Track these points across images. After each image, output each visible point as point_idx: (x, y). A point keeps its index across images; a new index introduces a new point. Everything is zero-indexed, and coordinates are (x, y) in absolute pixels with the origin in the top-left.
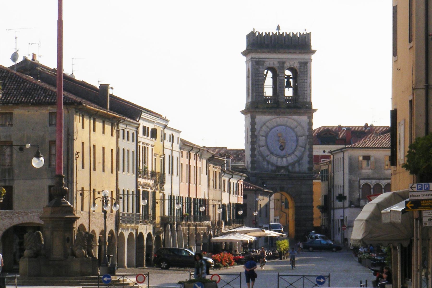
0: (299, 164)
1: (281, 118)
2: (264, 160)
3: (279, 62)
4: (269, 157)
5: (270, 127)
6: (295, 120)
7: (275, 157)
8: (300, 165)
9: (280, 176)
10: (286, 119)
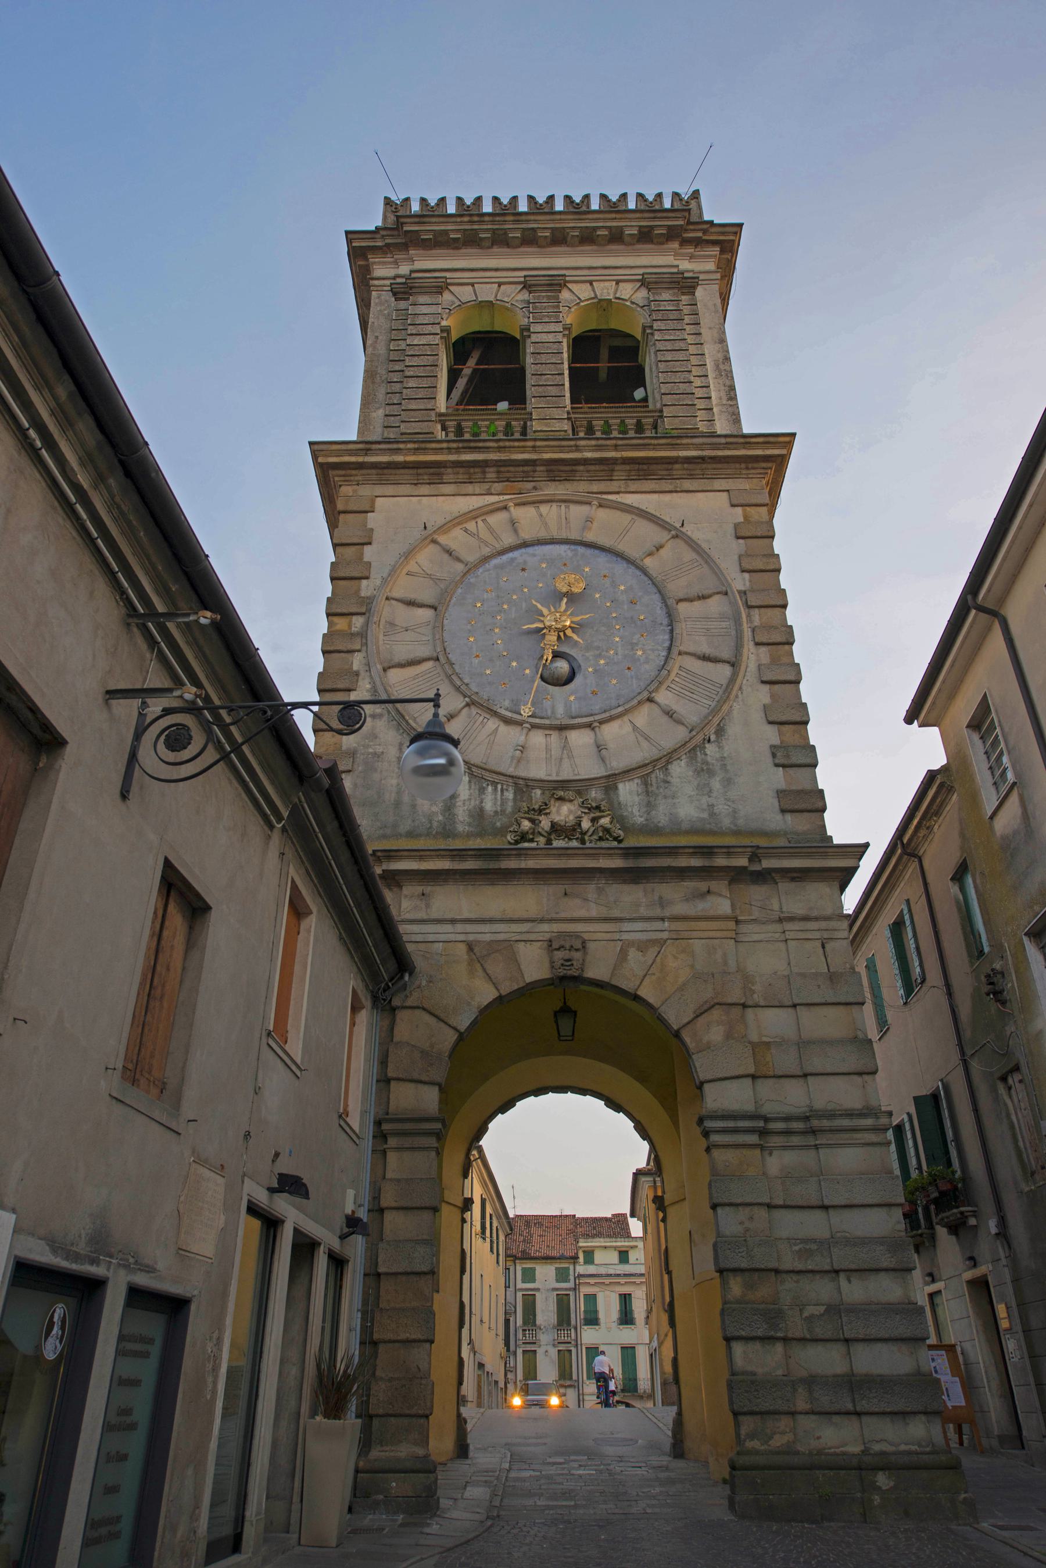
0: (704, 771)
1: (544, 509)
7: (503, 728)
8: (711, 773)
9: (549, 842)
10: (577, 512)
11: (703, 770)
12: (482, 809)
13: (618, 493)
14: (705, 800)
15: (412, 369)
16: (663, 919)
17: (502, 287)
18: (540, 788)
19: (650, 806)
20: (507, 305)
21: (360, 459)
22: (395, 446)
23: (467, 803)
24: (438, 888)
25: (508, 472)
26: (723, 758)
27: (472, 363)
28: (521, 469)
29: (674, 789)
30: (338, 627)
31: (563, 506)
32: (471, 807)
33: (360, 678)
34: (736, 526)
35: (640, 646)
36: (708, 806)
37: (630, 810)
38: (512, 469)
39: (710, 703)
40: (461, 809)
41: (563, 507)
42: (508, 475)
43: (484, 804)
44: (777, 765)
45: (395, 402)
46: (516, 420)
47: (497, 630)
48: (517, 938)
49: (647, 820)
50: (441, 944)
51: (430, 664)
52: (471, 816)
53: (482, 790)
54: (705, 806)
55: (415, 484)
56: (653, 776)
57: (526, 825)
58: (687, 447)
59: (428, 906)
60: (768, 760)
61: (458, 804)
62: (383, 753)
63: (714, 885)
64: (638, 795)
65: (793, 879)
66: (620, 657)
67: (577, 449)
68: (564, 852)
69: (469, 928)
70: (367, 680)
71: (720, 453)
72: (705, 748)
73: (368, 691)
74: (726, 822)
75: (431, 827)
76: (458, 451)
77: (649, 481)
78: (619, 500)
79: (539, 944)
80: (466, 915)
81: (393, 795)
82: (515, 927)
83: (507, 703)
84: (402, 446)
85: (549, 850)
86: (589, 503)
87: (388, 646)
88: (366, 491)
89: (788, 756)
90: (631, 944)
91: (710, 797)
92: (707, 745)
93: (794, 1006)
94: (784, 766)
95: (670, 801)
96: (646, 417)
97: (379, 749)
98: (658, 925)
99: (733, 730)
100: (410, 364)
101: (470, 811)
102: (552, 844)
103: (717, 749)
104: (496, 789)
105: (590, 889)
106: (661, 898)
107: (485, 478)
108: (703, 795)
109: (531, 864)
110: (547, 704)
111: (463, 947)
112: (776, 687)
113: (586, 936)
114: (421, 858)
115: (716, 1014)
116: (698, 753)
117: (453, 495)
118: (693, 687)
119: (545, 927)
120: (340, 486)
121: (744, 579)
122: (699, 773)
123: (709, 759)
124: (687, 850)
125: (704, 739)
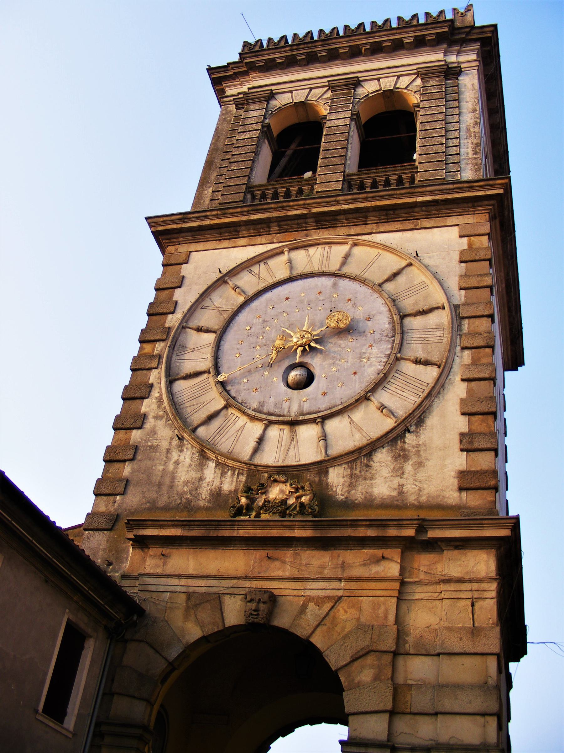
1: (312, 250)
2: (181, 439)
3: (332, 87)
4: (216, 423)
5: (251, 292)
6: (386, 248)
8: (406, 458)
9: (258, 515)
11: (399, 455)
12: (220, 489)
13: (370, 234)
14: (396, 481)
15: (236, 156)
16: (340, 580)
17: (313, 91)
18: (267, 472)
19: (352, 486)
20: (314, 102)
21: (179, 226)
22: (204, 214)
23: (210, 484)
24: (174, 551)
25: (286, 225)
26: (418, 446)
27: (293, 147)
28: (296, 222)
29: (373, 471)
30: (146, 351)
31: (327, 246)
32: (213, 487)
33: (153, 389)
34: (462, 253)
35: (367, 355)
36: (399, 485)
37: (334, 489)
38: (289, 222)
39: (416, 399)
40: (205, 489)
41: (327, 248)
42: (286, 227)
43: (222, 485)
44: (462, 450)
45: (221, 182)
46: (305, 185)
47: (258, 348)
48: (225, 592)
49: (346, 498)
50: (169, 593)
51: (206, 376)
52: (211, 494)
53: (223, 474)
54: (396, 486)
55: (220, 240)
56: (359, 461)
57: (243, 500)
58: (424, 194)
59: (164, 564)
60: (456, 445)
61: (204, 485)
62: (157, 445)
63: (388, 552)
64: (343, 477)
65: (457, 548)
66: (349, 364)
67: (338, 203)
68: (266, 524)
69: (191, 582)
70: (158, 390)
71: (450, 196)
72: (405, 436)
73: (156, 398)
74: (412, 499)
75: (180, 503)
76: (249, 213)
77: (396, 223)
78: (370, 240)
79: (241, 596)
80: (191, 571)
81: (158, 478)
82: (225, 583)
83: (255, 405)
84: (208, 213)
85: (258, 523)
86: (347, 244)
87: (178, 364)
88: (183, 249)
89: (471, 442)
90: (310, 599)
91: (401, 478)
92: (407, 435)
93: (438, 655)
94: (468, 451)
95: (368, 482)
96: (405, 173)
97: (156, 443)
98: (335, 584)
99: (432, 421)
100: (236, 153)
101: (211, 490)
102: (260, 517)
103: (415, 438)
104: (233, 474)
105: (288, 554)
106: (343, 562)
107: (270, 231)
108: (397, 476)
109: (242, 532)
110: (286, 405)
111: (183, 597)
112: (473, 384)
113: (276, 592)
114: (161, 527)
115: (370, 660)
116: (399, 441)
117: (246, 246)
118: (405, 387)
119: (247, 584)
120: (167, 246)
121: (460, 295)
122: (396, 458)
123: (406, 446)
124: (364, 523)
125: (405, 430)
